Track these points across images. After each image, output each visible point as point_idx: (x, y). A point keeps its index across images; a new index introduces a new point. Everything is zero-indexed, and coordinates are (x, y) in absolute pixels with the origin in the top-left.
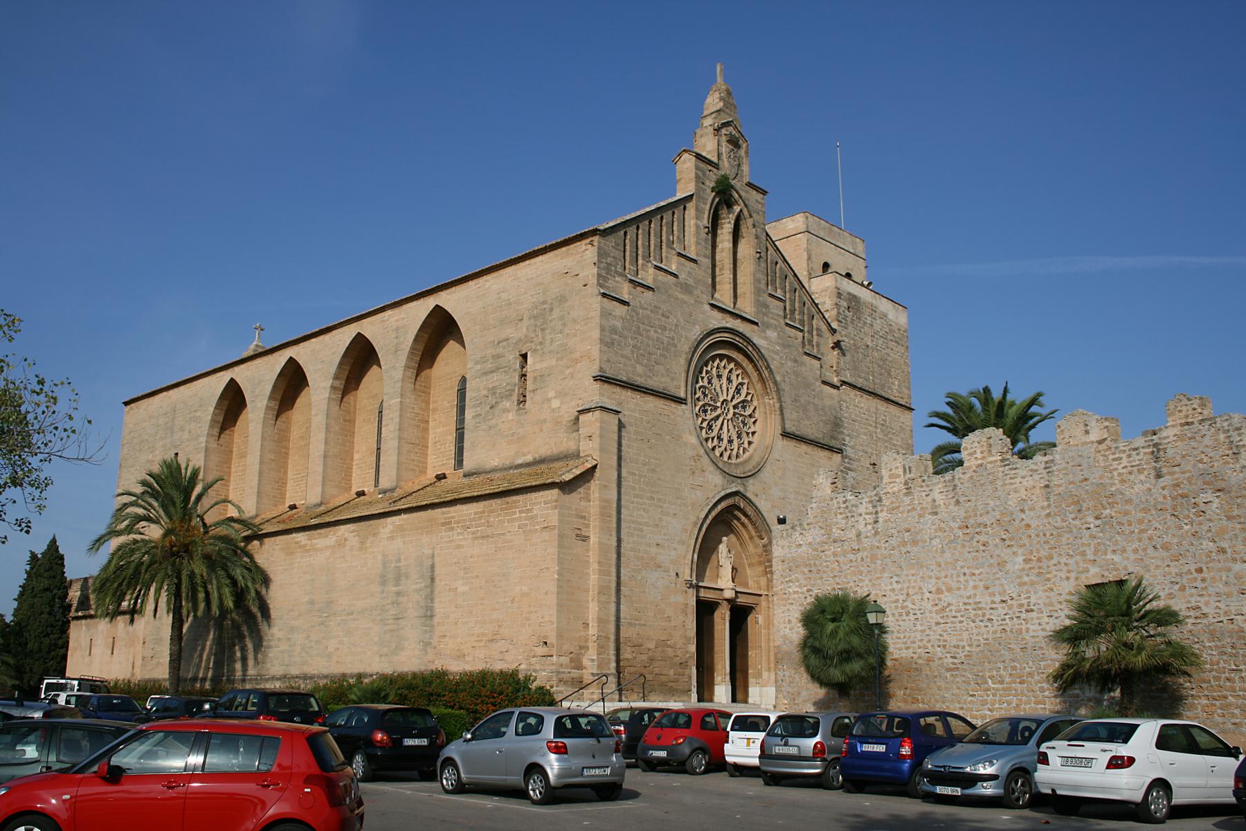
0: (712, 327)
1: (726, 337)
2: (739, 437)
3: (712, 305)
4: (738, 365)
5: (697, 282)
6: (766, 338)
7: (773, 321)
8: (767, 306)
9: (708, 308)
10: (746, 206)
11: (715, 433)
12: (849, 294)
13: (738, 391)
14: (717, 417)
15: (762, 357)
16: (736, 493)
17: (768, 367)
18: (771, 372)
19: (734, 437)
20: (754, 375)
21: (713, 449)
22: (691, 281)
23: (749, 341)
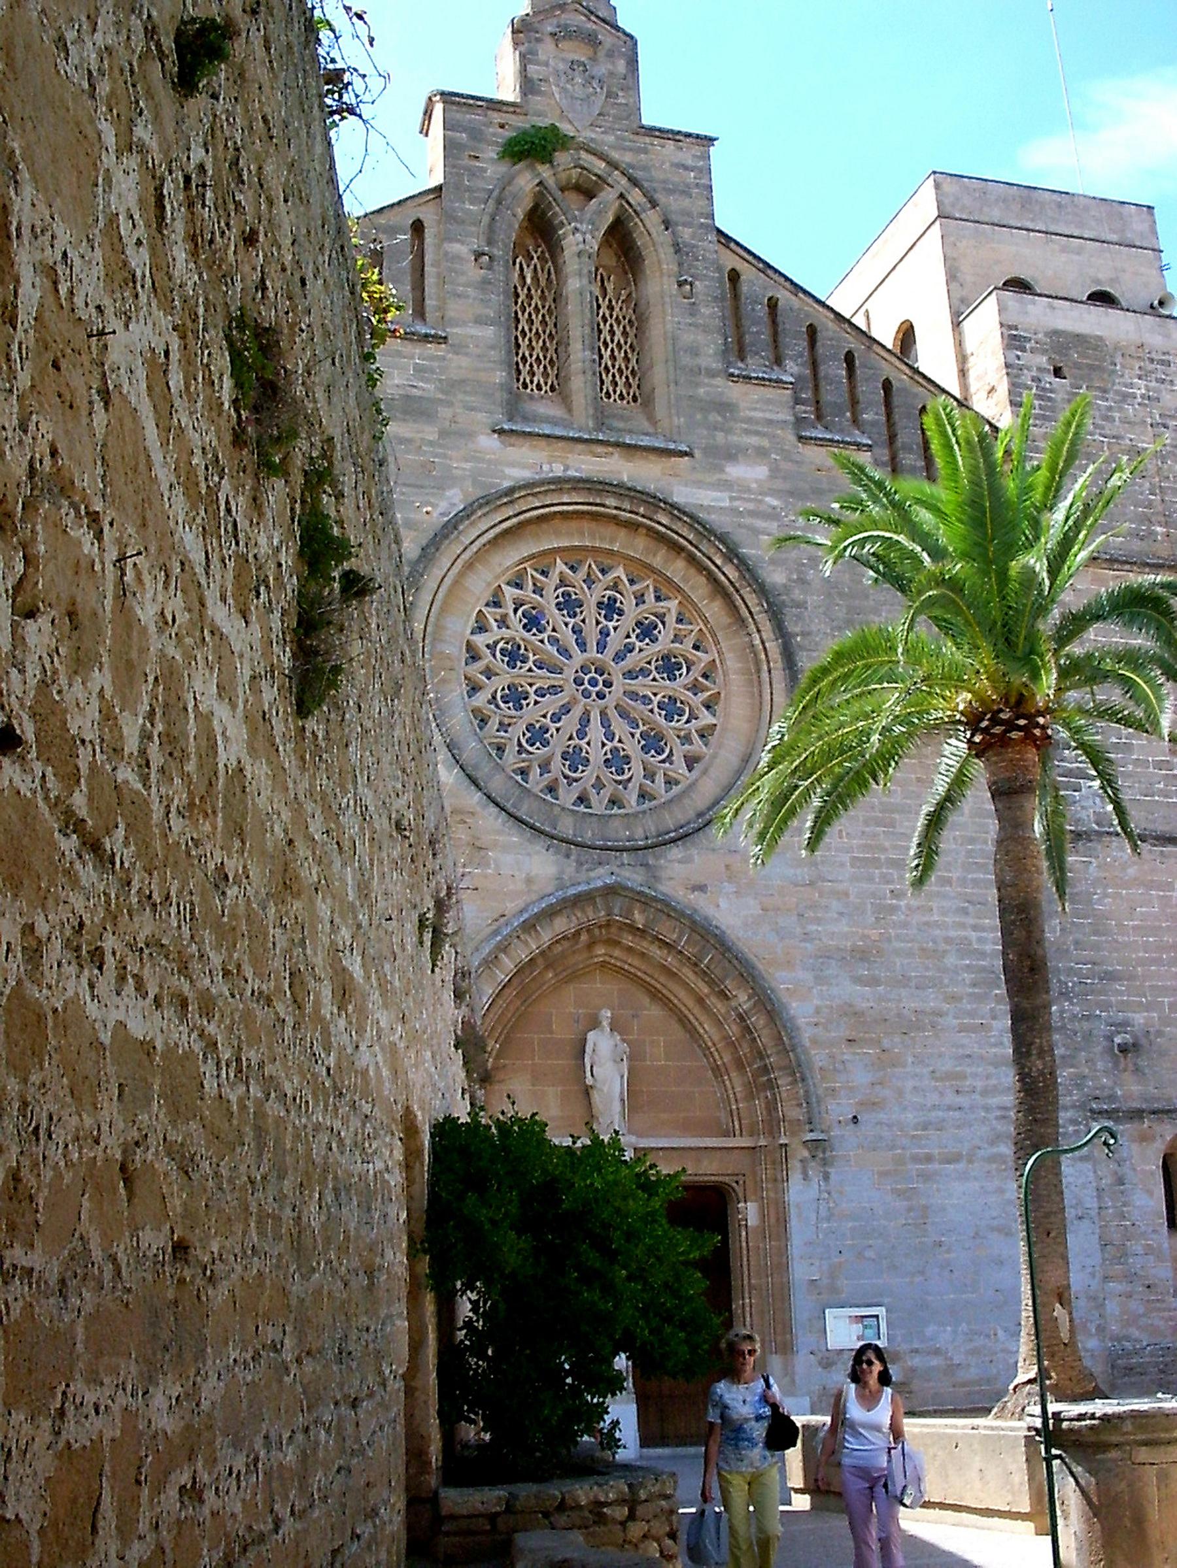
0: (507, 484)
1: (571, 500)
2: (653, 742)
3: (501, 432)
4: (639, 569)
5: (452, 386)
6: (726, 485)
7: (754, 440)
8: (725, 407)
9: (489, 442)
10: (634, 182)
11: (558, 743)
12: (1056, 333)
13: (647, 631)
14: (566, 709)
15: (706, 531)
16: (610, 891)
17: (733, 554)
18: (743, 565)
19: (632, 748)
20: (697, 587)
21: (551, 789)
22: (427, 388)
23: (655, 501)
